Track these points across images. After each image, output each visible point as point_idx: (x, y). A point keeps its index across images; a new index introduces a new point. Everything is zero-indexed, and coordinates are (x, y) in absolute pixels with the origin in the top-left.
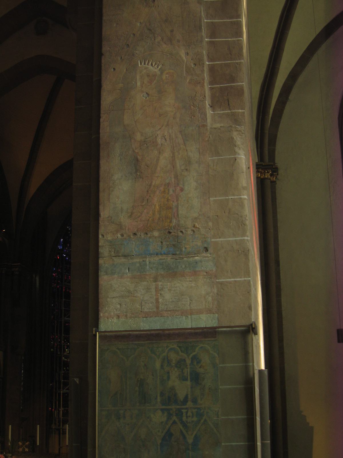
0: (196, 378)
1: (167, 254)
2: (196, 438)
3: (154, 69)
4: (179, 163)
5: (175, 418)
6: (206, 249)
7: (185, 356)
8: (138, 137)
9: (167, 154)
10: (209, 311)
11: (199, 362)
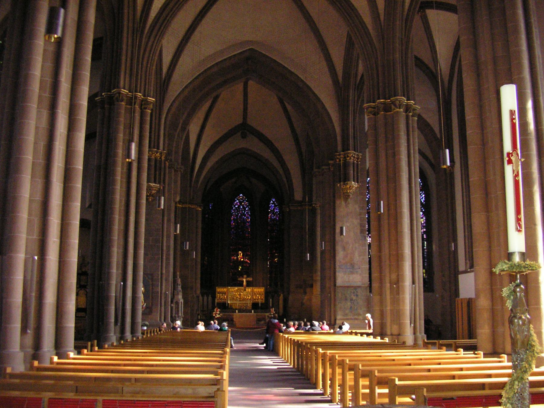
0: (357, 295)
1: (351, 269)
2: (357, 308)
3: (348, 225)
4: (354, 248)
5: (353, 304)
6: (359, 268)
7: (354, 291)
8: (345, 241)
9: (351, 245)
10: (360, 282)
11: (358, 293)
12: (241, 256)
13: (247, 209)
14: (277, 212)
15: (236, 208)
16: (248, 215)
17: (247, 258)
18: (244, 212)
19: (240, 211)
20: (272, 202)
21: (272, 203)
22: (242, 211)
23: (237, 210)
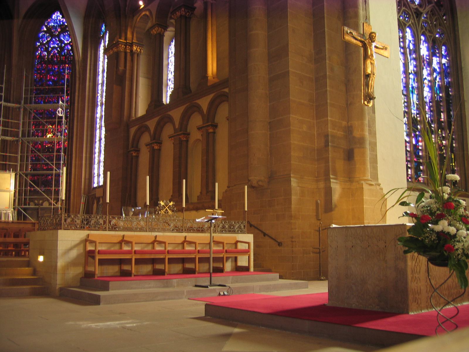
20: (45, 29)
21: (44, 31)
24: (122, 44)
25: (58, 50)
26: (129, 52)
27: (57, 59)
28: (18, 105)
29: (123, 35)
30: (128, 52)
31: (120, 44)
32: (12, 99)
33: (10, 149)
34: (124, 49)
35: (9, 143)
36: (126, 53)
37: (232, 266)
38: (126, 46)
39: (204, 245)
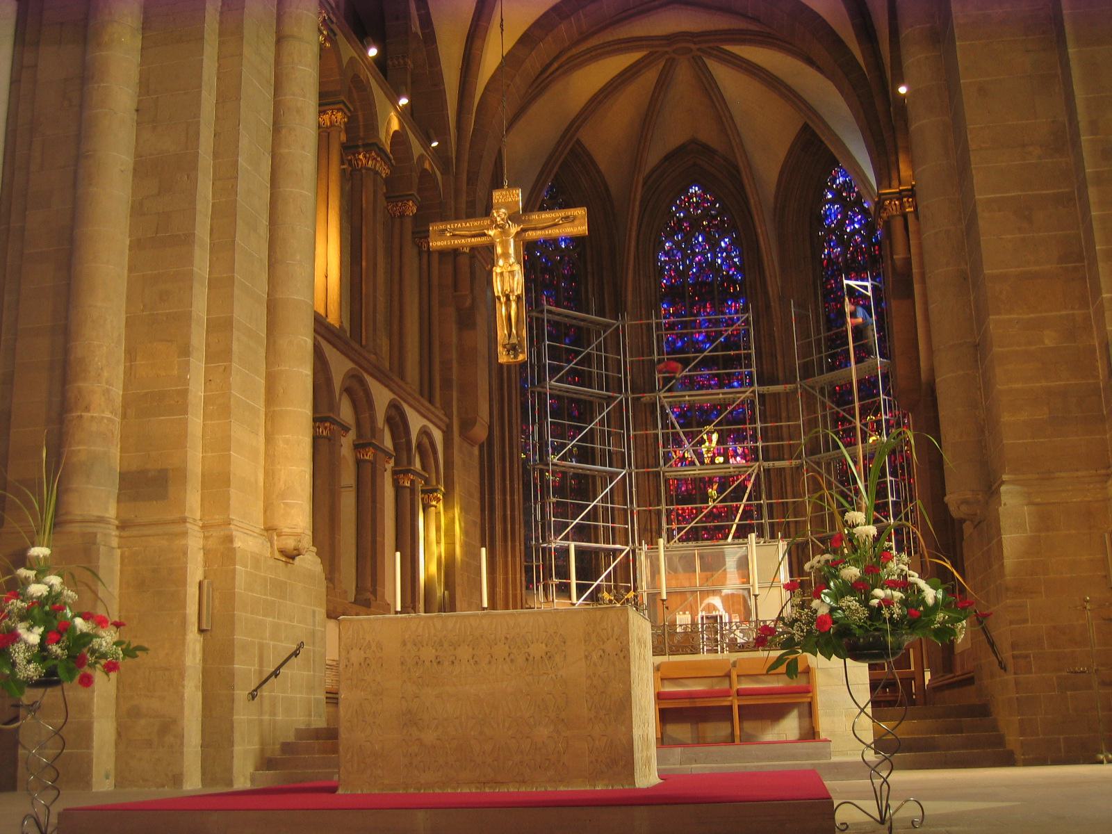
12: (714, 444)
13: (723, 244)
14: (854, 232)
15: (678, 244)
16: (730, 267)
17: (740, 451)
18: (715, 257)
19: (695, 254)
20: (830, 196)
22: (703, 254)
23: (683, 251)
24: (891, 200)
25: (861, 235)
26: (911, 212)
27: (864, 257)
28: (789, 387)
29: (894, 175)
30: (908, 212)
31: (886, 200)
32: (781, 375)
33: (793, 486)
34: (898, 208)
35: (788, 472)
36: (905, 216)
37: (800, 728)
38: (900, 199)
39: (714, 680)
